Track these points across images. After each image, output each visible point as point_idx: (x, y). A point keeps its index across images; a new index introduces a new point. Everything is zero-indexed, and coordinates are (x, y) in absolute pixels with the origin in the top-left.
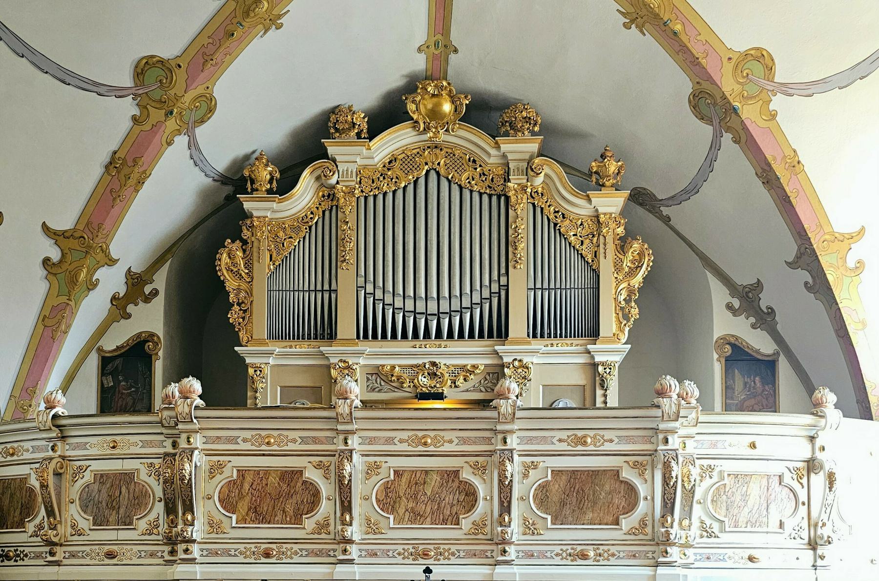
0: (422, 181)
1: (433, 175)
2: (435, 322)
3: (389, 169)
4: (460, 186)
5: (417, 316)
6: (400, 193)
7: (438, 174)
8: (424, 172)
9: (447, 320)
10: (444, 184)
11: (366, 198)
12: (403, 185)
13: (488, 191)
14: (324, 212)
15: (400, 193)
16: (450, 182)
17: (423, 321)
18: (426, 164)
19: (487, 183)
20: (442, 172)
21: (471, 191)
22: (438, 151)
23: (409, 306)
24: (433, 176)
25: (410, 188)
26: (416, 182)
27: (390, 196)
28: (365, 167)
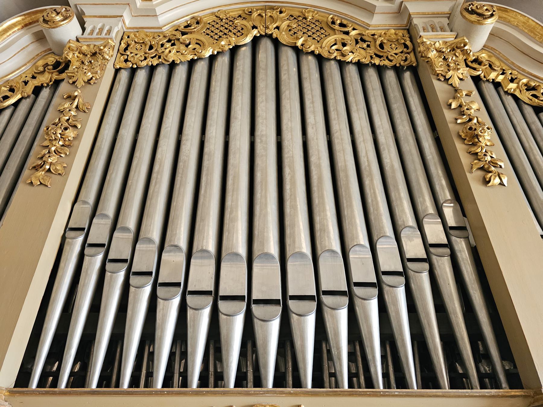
0: (245, 54)
1: (266, 51)
2: (275, 326)
3: (183, 34)
4: (320, 60)
5: (223, 306)
6: (201, 69)
7: (277, 43)
8: (248, 39)
9: (311, 321)
10: (288, 58)
11: (133, 72)
12: (208, 53)
13: (377, 61)
14: (37, 91)
15: (201, 69)
16: (298, 52)
17: (239, 322)
18: (254, 27)
19: (371, 51)
20: (284, 38)
21: (342, 65)
22: (275, 14)
23: (202, 276)
24: (266, 51)
25: (223, 62)
26: (234, 51)
27: (181, 73)
28: (139, 29)
